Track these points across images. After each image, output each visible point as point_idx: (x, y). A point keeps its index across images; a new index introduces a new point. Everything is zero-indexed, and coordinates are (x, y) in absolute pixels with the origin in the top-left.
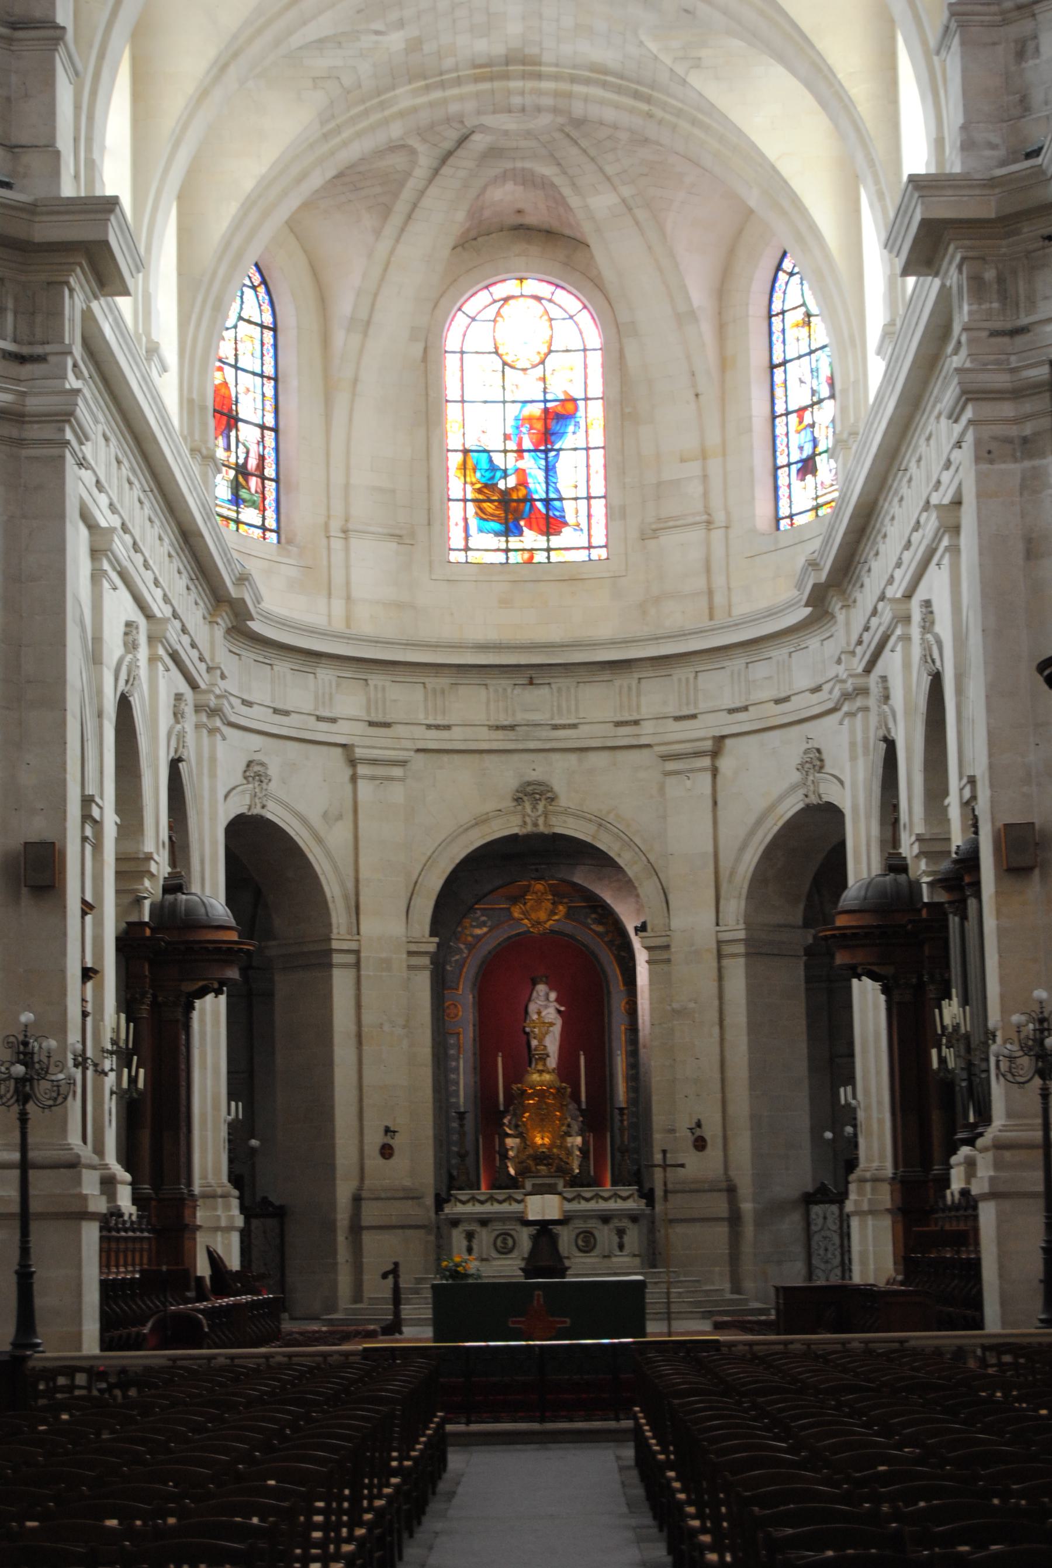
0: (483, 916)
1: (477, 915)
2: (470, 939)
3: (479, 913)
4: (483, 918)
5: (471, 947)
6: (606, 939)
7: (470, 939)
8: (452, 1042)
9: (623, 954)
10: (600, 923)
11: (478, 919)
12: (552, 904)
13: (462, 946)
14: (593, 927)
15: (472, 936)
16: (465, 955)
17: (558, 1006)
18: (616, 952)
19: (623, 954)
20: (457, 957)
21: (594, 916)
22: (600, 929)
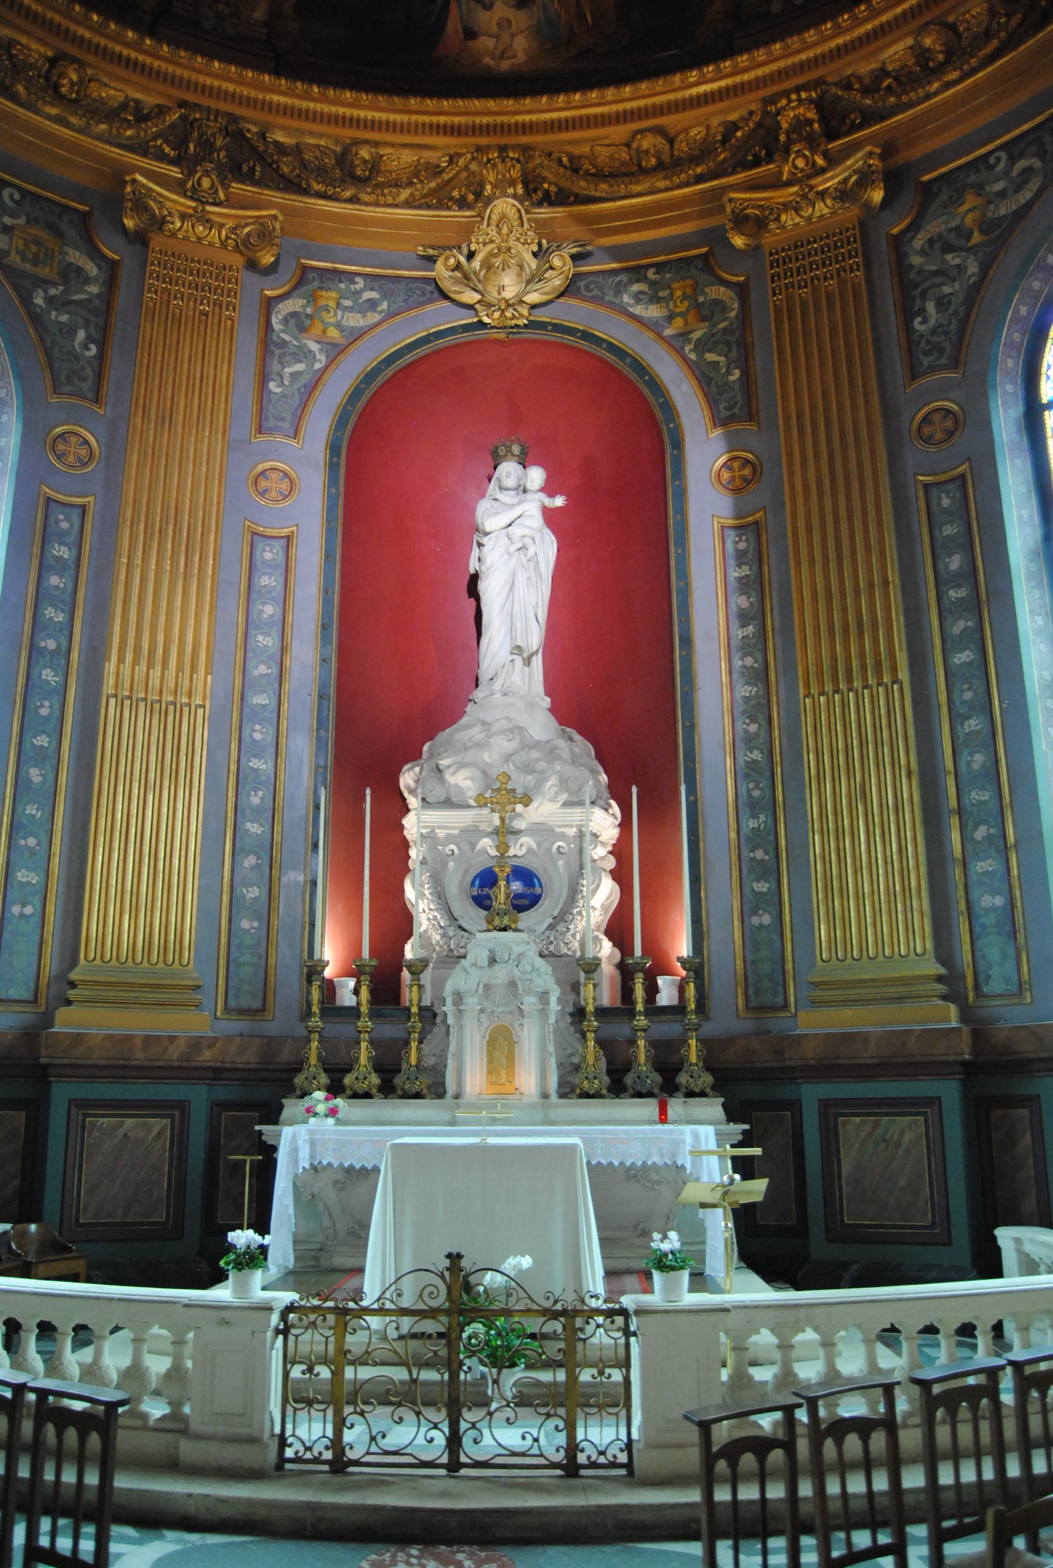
0: (372, 289)
1: (357, 287)
2: (333, 333)
3: (360, 282)
4: (373, 295)
5: (336, 352)
6: (668, 332)
7: (333, 333)
8: (268, 556)
9: (710, 357)
10: (655, 299)
11: (358, 293)
12: (535, 255)
13: (314, 346)
14: (637, 310)
15: (339, 326)
16: (317, 366)
17: (548, 502)
18: (693, 356)
19: (710, 357)
20: (300, 367)
21: (636, 287)
22: (653, 312)
